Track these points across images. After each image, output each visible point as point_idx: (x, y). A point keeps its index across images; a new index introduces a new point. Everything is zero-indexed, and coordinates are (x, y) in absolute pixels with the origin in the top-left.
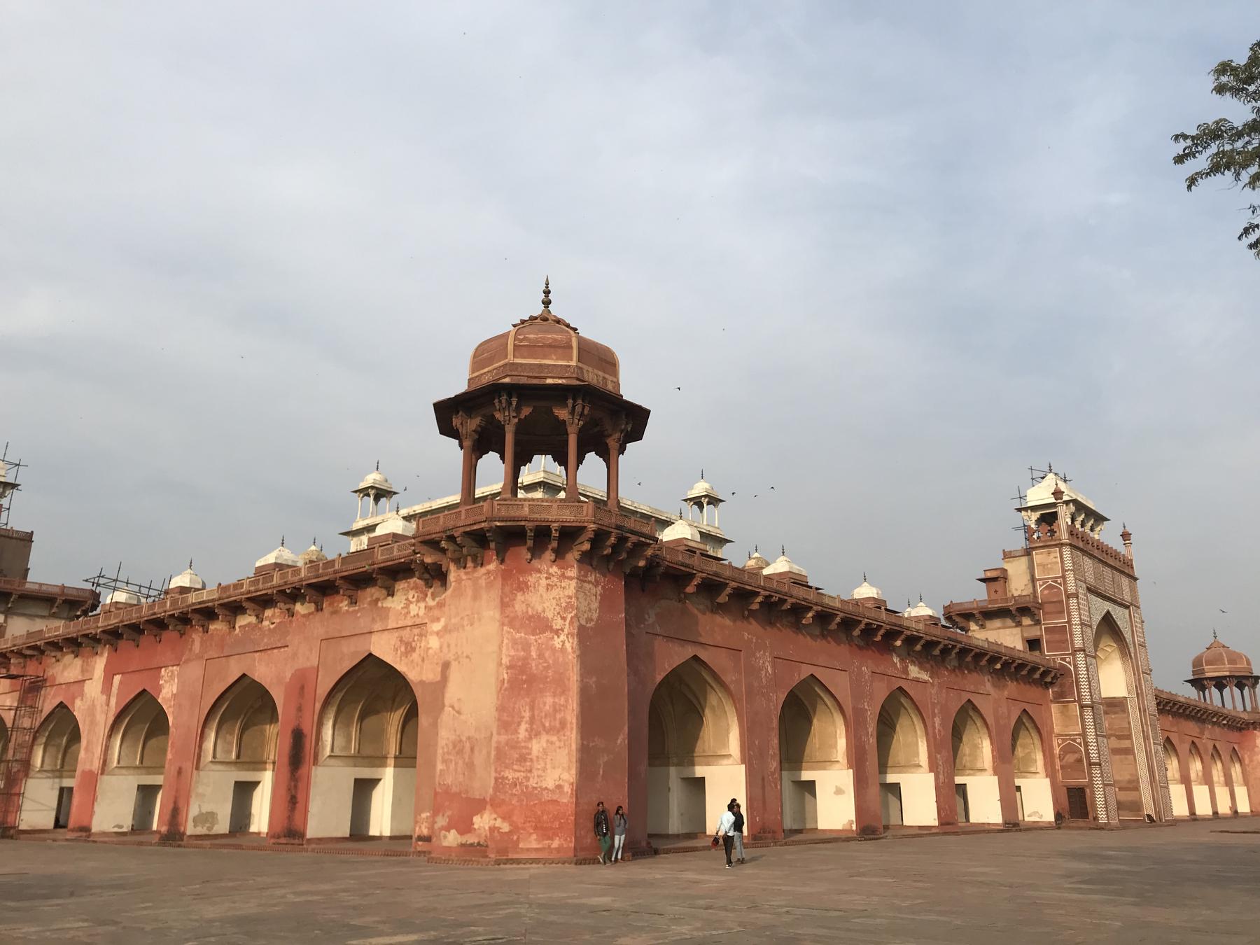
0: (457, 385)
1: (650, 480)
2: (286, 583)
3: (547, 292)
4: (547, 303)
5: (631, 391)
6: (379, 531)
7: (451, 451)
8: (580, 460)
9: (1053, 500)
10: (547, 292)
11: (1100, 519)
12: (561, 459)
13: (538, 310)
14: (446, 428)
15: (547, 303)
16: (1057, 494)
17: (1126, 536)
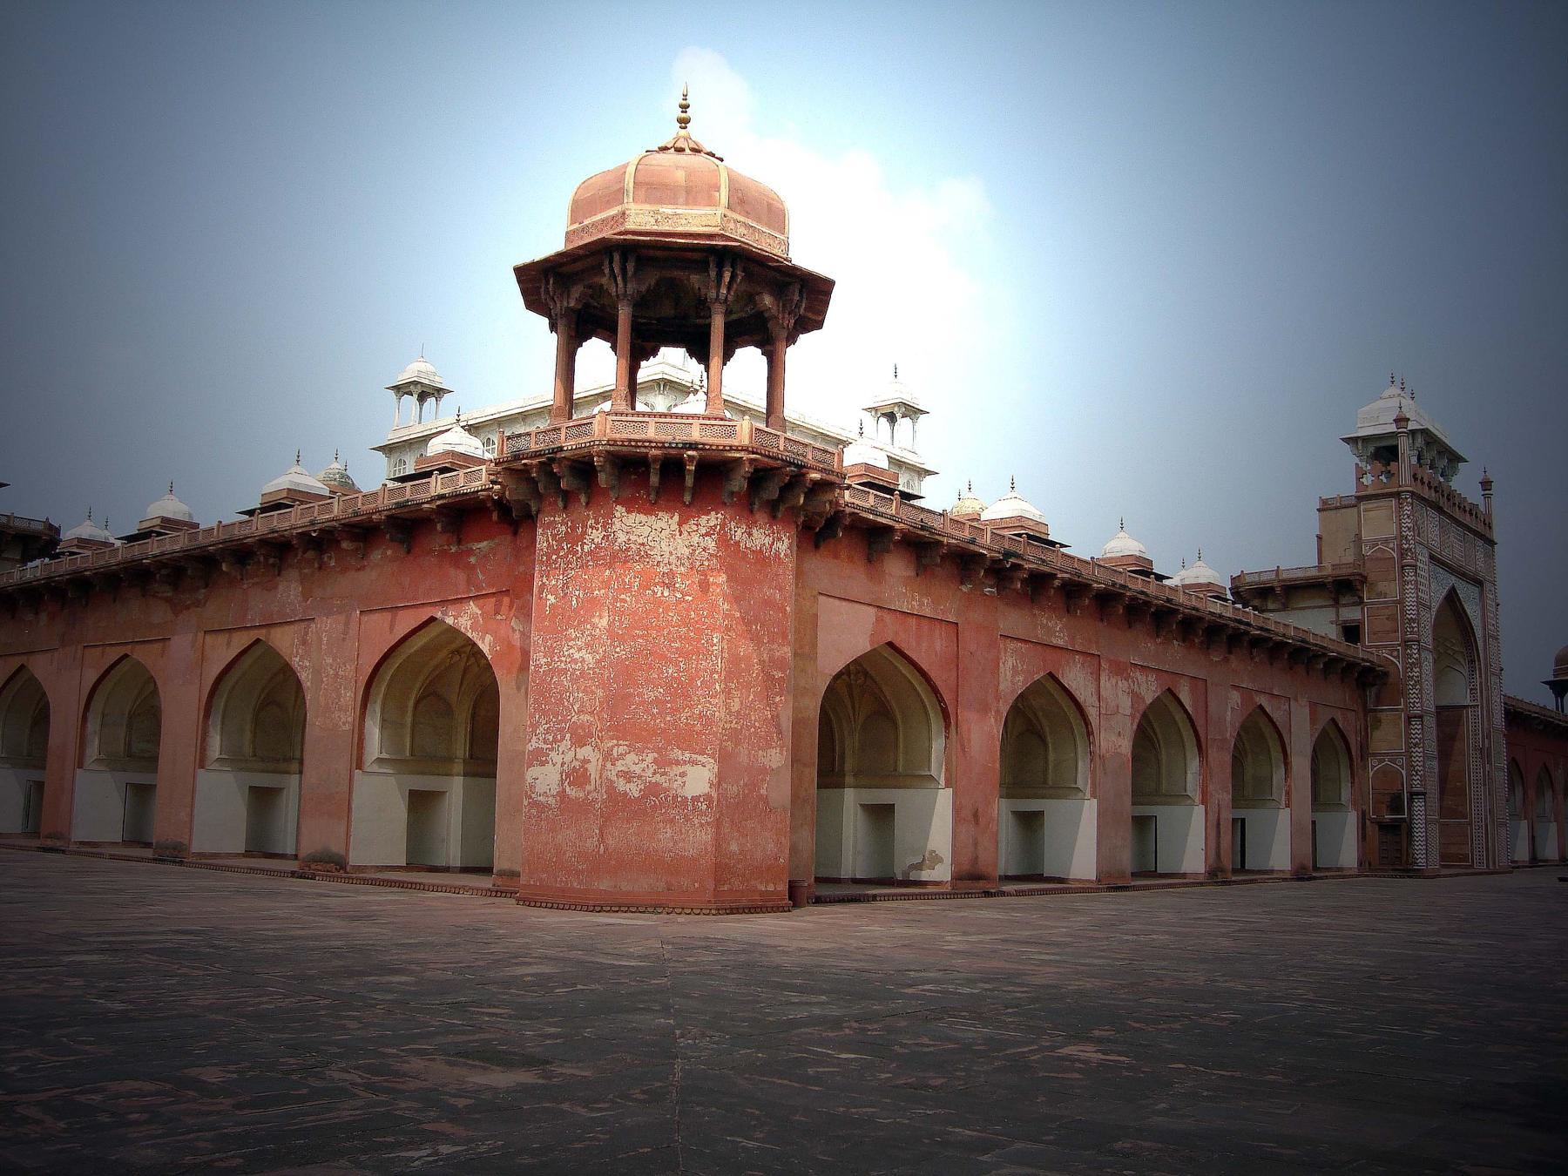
0: (548, 240)
1: (826, 390)
2: (312, 523)
3: (685, 108)
4: (684, 122)
5: (804, 254)
6: (435, 447)
7: (540, 336)
8: (727, 356)
9: (1393, 428)
10: (685, 108)
11: (1455, 459)
12: (700, 352)
13: (669, 132)
14: (534, 302)
15: (684, 122)
16: (1401, 420)
17: (1486, 485)
